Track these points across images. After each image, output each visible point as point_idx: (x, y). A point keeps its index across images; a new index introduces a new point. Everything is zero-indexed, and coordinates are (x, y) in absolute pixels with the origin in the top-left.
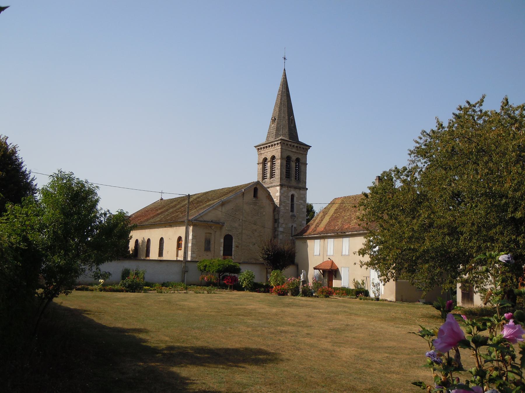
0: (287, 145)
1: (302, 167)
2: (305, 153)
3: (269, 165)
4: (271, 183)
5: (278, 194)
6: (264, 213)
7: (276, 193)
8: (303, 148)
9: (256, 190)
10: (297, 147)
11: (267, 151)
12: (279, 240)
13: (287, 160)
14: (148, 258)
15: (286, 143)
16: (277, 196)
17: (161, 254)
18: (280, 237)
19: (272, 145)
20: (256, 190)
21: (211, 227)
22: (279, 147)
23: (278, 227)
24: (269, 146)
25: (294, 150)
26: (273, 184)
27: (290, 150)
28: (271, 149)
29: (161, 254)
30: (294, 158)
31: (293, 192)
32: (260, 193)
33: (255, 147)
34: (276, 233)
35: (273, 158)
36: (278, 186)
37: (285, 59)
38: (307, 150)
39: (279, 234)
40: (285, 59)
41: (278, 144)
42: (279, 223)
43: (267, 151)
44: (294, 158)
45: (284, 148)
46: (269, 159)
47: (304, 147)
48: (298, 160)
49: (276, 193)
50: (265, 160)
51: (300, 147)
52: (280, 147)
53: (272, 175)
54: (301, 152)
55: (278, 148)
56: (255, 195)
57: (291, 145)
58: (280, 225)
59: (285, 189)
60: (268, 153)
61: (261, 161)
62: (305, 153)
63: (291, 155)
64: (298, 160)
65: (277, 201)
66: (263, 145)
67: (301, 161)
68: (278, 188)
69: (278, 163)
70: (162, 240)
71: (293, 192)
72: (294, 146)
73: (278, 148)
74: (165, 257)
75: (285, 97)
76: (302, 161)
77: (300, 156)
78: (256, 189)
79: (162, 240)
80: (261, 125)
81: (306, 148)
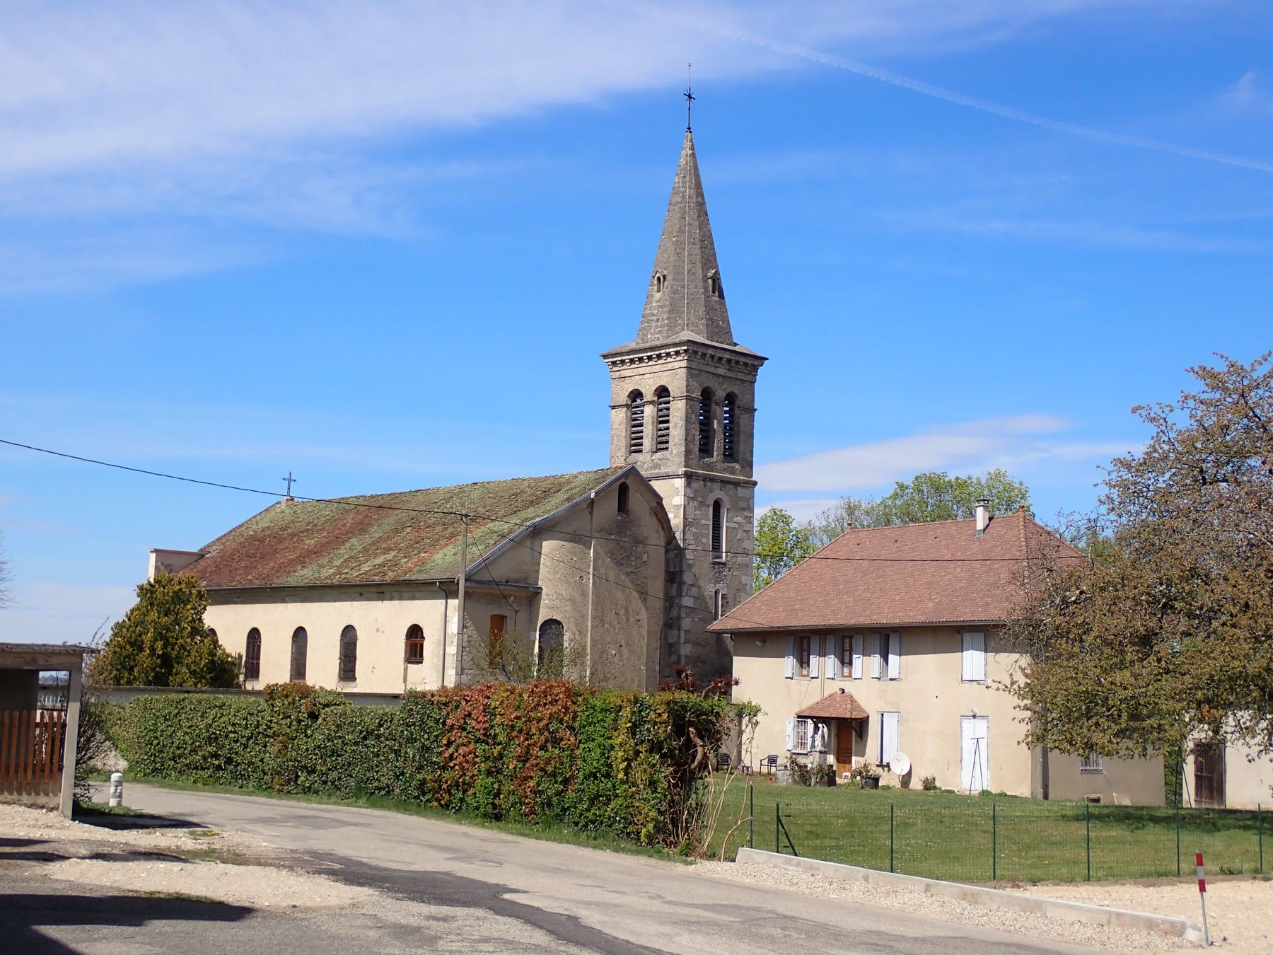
0: (704, 355)
1: (743, 419)
2: (749, 378)
3: (649, 411)
4: (657, 466)
5: (679, 500)
6: (645, 558)
7: (673, 494)
8: (746, 365)
9: (623, 490)
10: (729, 361)
11: (642, 371)
12: (682, 634)
13: (704, 402)
14: (350, 688)
15: (701, 350)
16: (678, 507)
17: (348, 671)
18: (686, 623)
19: (659, 357)
20: (623, 490)
21: (505, 597)
22: (681, 363)
23: (680, 595)
24: (650, 358)
25: (721, 371)
26: (663, 470)
27: (712, 369)
28: (654, 366)
29: (348, 671)
30: (720, 394)
31: (718, 494)
32: (636, 501)
33: (605, 357)
34: (674, 613)
35: (662, 392)
36: (678, 476)
37: (689, 96)
38: (755, 368)
39: (683, 614)
40: (689, 96)
41: (677, 353)
42: (682, 583)
43: (642, 371)
44: (720, 394)
45: (694, 365)
46: (649, 395)
47: (748, 361)
48: (731, 399)
49: (673, 494)
50: (636, 395)
51: (737, 362)
52: (684, 364)
53: (662, 443)
54: (740, 376)
55: (676, 365)
56: (623, 507)
57: (712, 357)
58: (685, 588)
59: (697, 485)
60: (647, 379)
61: (623, 398)
62: (749, 378)
63: (712, 383)
64: (731, 399)
65: (676, 520)
66: (628, 353)
67: (737, 403)
68: (680, 483)
69: (678, 409)
70: (300, 635)
71: (718, 494)
72: (720, 359)
73: (676, 365)
74: (363, 684)
75: (694, 214)
76: (742, 401)
77: (736, 389)
78: (627, 489)
79: (300, 635)
80: (640, 307)
81: (752, 363)
